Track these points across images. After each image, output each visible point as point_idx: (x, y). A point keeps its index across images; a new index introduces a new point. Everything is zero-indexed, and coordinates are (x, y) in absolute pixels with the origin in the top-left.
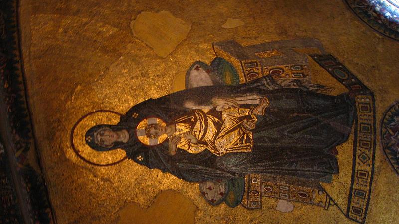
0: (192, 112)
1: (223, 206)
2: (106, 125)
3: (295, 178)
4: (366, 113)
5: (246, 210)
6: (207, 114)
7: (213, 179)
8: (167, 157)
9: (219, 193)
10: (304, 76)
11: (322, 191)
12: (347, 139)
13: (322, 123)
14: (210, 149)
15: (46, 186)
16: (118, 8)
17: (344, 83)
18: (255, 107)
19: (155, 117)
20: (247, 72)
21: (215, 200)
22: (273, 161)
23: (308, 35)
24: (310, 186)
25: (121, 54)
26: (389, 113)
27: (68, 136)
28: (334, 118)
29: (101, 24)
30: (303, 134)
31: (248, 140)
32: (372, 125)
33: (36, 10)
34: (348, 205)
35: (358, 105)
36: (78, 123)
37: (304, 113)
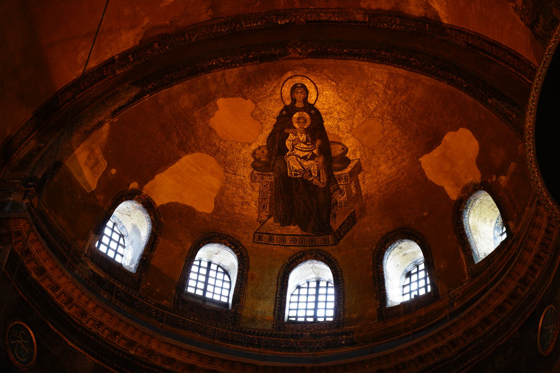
0: (313, 143)
1: (252, 160)
6: (313, 152)
7: (269, 154)
9: (260, 157)
10: (340, 207)
12: (304, 231)
13: (311, 216)
15: (274, 61)
16: (386, 114)
17: (340, 229)
18: (318, 179)
21: (256, 154)
26: (325, 254)
27: (303, 74)
29: (377, 103)
31: (296, 175)
32: (315, 245)
33: (391, 74)
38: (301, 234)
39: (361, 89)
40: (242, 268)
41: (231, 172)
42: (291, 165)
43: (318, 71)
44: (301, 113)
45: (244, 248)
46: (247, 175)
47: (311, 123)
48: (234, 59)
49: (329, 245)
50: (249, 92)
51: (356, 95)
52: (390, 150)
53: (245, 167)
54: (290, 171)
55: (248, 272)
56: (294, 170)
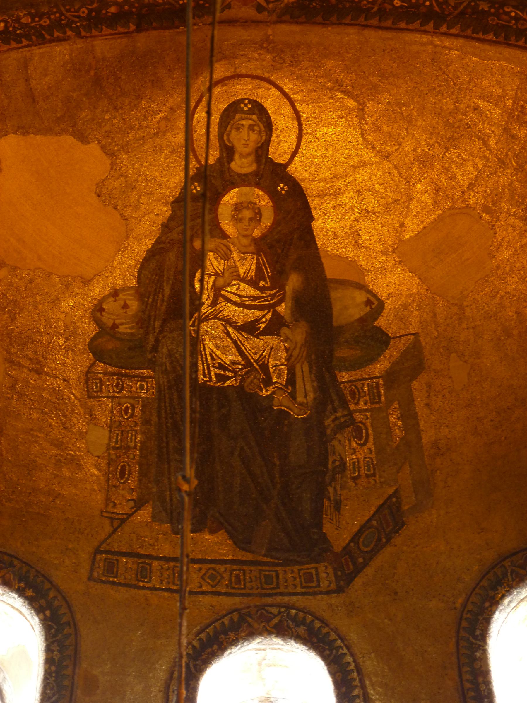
7: (143, 311)
9: (117, 322)
10: (354, 479)
12: (243, 549)
13: (265, 506)
15: (178, 27)
16: (507, 197)
17: (352, 544)
18: (289, 393)
19: (274, 221)
20: (361, 386)
21: (103, 313)
25: (414, 184)
27: (259, 72)
29: (480, 166)
31: (222, 378)
32: (278, 591)
34: (117, 552)
35: (312, 568)
38: (235, 558)
39: (434, 122)
40: (59, 656)
41: (27, 363)
42: (207, 350)
43: (306, 63)
44: (246, 189)
45: (64, 598)
46: (73, 376)
47: (276, 224)
48: (62, 14)
49: (321, 593)
50: (95, 122)
51: (418, 141)
52: (514, 309)
53: (70, 352)
54: (203, 366)
55: (74, 668)
56: (216, 365)
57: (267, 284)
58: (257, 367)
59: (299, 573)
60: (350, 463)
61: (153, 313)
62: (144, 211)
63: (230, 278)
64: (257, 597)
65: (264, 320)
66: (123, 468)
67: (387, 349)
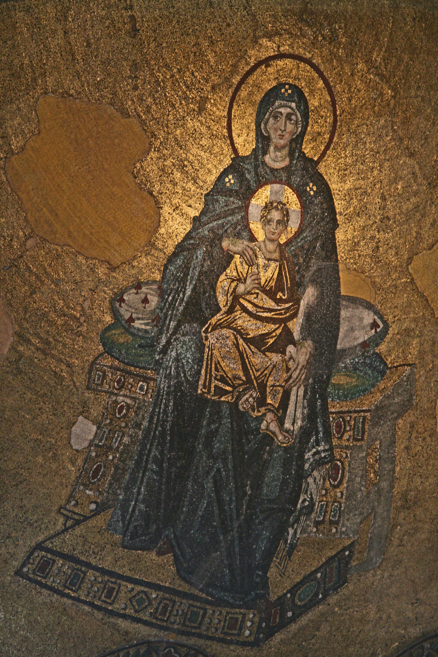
1: (108, 319)
2: (306, 129)
3: (131, 464)
4: (222, 623)
5: (91, 358)
6: (286, 326)
7: (161, 310)
8: (221, 232)
9: (134, 316)
10: (317, 524)
11: (96, 509)
14: (218, 316)
17: (289, 595)
20: (349, 418)
22: (171, 430)
23: (393, 549)
24: (109, 488)
28: (226, 562)
30: (210, 497)
32: (198, 631)
34: (59, 552)
36: (321, 75)
37: (248, 508)
38: (171, 586)
42: (214, 359)
44: (276, 186)
49: (237, 643)
50: (136, 93)
54: (206, 376)
57: (284, 296)
58: (256, 385)
59: (226, 617)
60: (318, 506)
61: (170, 312)
62: (177, 200)
63: (251, 286)
64: (174, 632)
65: (274, 334)
66: (98, 469)
67: (382, 380)
